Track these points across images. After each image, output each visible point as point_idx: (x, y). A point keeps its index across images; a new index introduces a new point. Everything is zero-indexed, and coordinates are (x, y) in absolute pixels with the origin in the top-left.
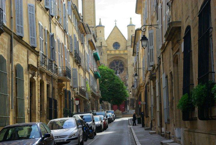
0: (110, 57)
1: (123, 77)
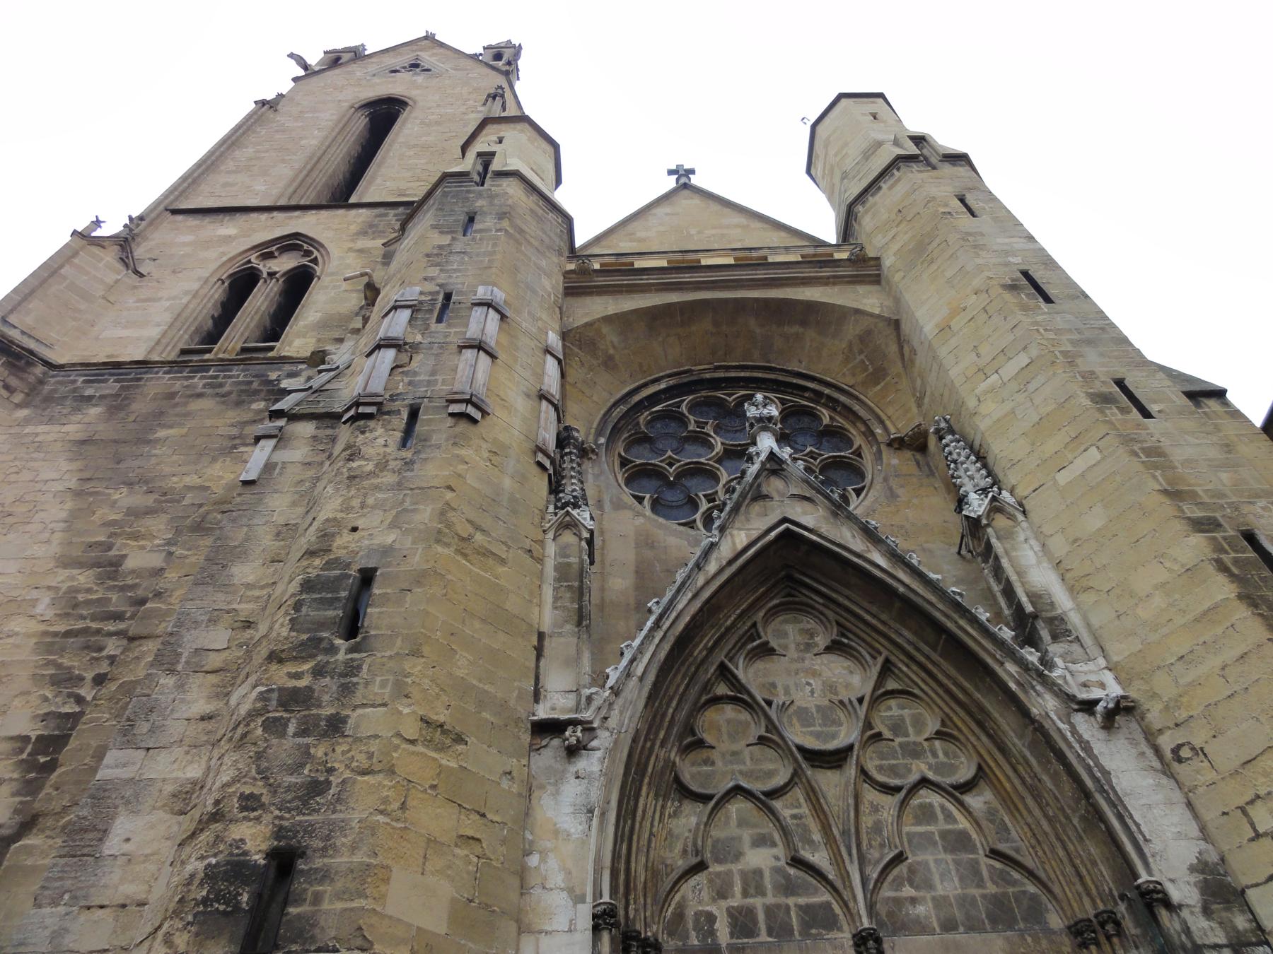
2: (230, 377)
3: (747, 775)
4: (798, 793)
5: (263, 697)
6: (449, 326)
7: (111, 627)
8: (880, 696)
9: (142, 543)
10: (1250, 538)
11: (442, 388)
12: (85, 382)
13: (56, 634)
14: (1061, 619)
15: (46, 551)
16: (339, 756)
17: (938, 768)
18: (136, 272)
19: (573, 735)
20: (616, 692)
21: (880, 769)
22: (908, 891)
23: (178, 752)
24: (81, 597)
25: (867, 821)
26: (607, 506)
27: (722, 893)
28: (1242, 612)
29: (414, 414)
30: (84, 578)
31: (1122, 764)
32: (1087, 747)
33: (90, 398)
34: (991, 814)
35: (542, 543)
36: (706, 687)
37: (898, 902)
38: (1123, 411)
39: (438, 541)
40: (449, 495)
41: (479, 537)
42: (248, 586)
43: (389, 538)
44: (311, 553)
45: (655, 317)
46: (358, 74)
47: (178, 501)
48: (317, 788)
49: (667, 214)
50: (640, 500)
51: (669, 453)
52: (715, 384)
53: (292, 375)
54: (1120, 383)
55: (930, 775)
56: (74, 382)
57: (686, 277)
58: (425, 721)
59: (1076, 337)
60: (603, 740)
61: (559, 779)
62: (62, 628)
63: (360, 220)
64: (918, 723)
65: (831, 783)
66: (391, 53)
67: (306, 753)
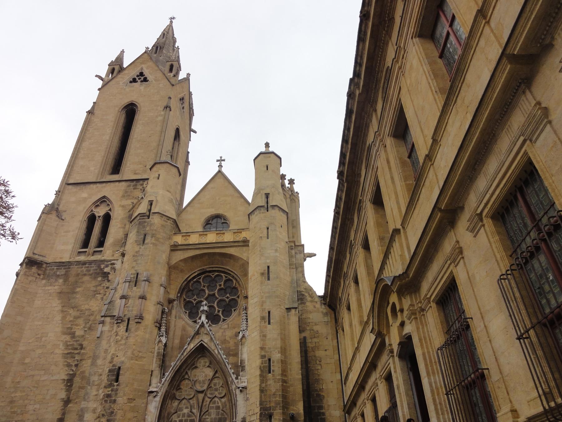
0: (180, 256)
1: (229, 334)
2: (91, 267)
3: (187, 395)
4: (195, 399)
5: (104, 395)
6: (137, 288)
7: (76, 352)
8: (214, 377)
9: (79, 327)
10: (270, 360)
11: (135, 313)
12: (57, 269)
13: (65, 354)
14: (244, 366)
15: (59, 329)
16: (115, 407)
17: (220, 393)
18: (62, 219)
19: (154, 394)
20: (163, 384)
21: (210, 394)
22: (207, 417)
23: (92, 402)
24: (69, 343)
25: (204, 404)
26: (177, 317)
27: (179, 417)
28: (258, 379)
29: (129, 320)
30: (68, 338)
31: (240, 398)
32: (236, 395)
33: (59, 276)
34: (225, 402)
35: (154, 348)
36: (184, 376)
37: (205, 418)
38: (265, 322)
39: (132, 360)
40: (134, 347)
41: (140, 354)
42: (100, 365)
43: (123, 359)
44: (110, 363)
45: (193, 258)
46: (121, 83)
47: (84, 314)
48: (112, 413)
49: (212, 188)
50: (186, 313)
51: (195, 297)
52: (210, 272)
53: (107, 266)
54: (269, 312)
55: (218, 395)
56: (54, 269)
57: (201, 246)
58: (129, 399)
59: (267, 295)
60: (160, 394)
61: (152, 401)
62: (66, 352)
63: (123, 188)
64: (219, 384)
65: (201, 396)
66: (133, 65)
67: (110, 406)
